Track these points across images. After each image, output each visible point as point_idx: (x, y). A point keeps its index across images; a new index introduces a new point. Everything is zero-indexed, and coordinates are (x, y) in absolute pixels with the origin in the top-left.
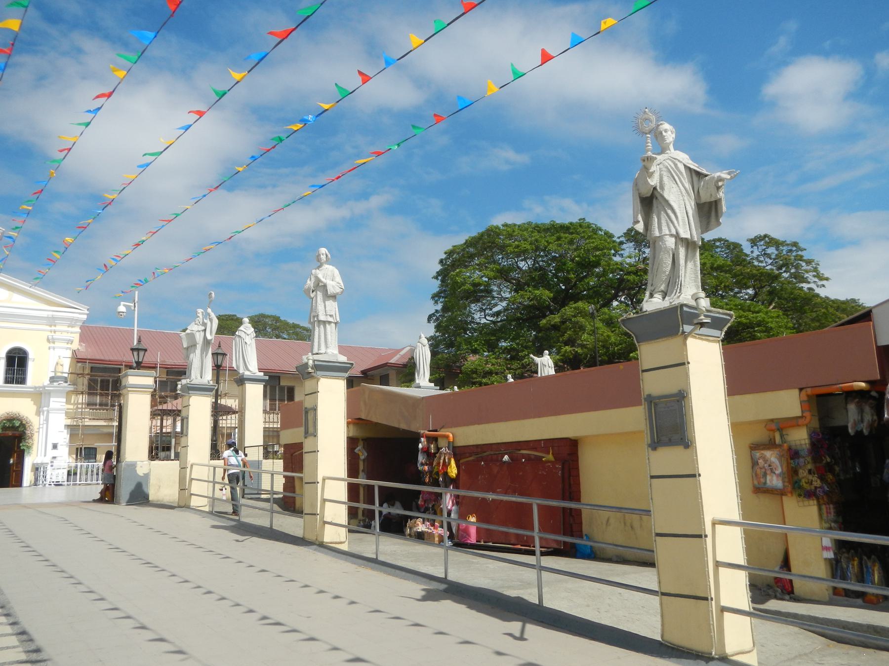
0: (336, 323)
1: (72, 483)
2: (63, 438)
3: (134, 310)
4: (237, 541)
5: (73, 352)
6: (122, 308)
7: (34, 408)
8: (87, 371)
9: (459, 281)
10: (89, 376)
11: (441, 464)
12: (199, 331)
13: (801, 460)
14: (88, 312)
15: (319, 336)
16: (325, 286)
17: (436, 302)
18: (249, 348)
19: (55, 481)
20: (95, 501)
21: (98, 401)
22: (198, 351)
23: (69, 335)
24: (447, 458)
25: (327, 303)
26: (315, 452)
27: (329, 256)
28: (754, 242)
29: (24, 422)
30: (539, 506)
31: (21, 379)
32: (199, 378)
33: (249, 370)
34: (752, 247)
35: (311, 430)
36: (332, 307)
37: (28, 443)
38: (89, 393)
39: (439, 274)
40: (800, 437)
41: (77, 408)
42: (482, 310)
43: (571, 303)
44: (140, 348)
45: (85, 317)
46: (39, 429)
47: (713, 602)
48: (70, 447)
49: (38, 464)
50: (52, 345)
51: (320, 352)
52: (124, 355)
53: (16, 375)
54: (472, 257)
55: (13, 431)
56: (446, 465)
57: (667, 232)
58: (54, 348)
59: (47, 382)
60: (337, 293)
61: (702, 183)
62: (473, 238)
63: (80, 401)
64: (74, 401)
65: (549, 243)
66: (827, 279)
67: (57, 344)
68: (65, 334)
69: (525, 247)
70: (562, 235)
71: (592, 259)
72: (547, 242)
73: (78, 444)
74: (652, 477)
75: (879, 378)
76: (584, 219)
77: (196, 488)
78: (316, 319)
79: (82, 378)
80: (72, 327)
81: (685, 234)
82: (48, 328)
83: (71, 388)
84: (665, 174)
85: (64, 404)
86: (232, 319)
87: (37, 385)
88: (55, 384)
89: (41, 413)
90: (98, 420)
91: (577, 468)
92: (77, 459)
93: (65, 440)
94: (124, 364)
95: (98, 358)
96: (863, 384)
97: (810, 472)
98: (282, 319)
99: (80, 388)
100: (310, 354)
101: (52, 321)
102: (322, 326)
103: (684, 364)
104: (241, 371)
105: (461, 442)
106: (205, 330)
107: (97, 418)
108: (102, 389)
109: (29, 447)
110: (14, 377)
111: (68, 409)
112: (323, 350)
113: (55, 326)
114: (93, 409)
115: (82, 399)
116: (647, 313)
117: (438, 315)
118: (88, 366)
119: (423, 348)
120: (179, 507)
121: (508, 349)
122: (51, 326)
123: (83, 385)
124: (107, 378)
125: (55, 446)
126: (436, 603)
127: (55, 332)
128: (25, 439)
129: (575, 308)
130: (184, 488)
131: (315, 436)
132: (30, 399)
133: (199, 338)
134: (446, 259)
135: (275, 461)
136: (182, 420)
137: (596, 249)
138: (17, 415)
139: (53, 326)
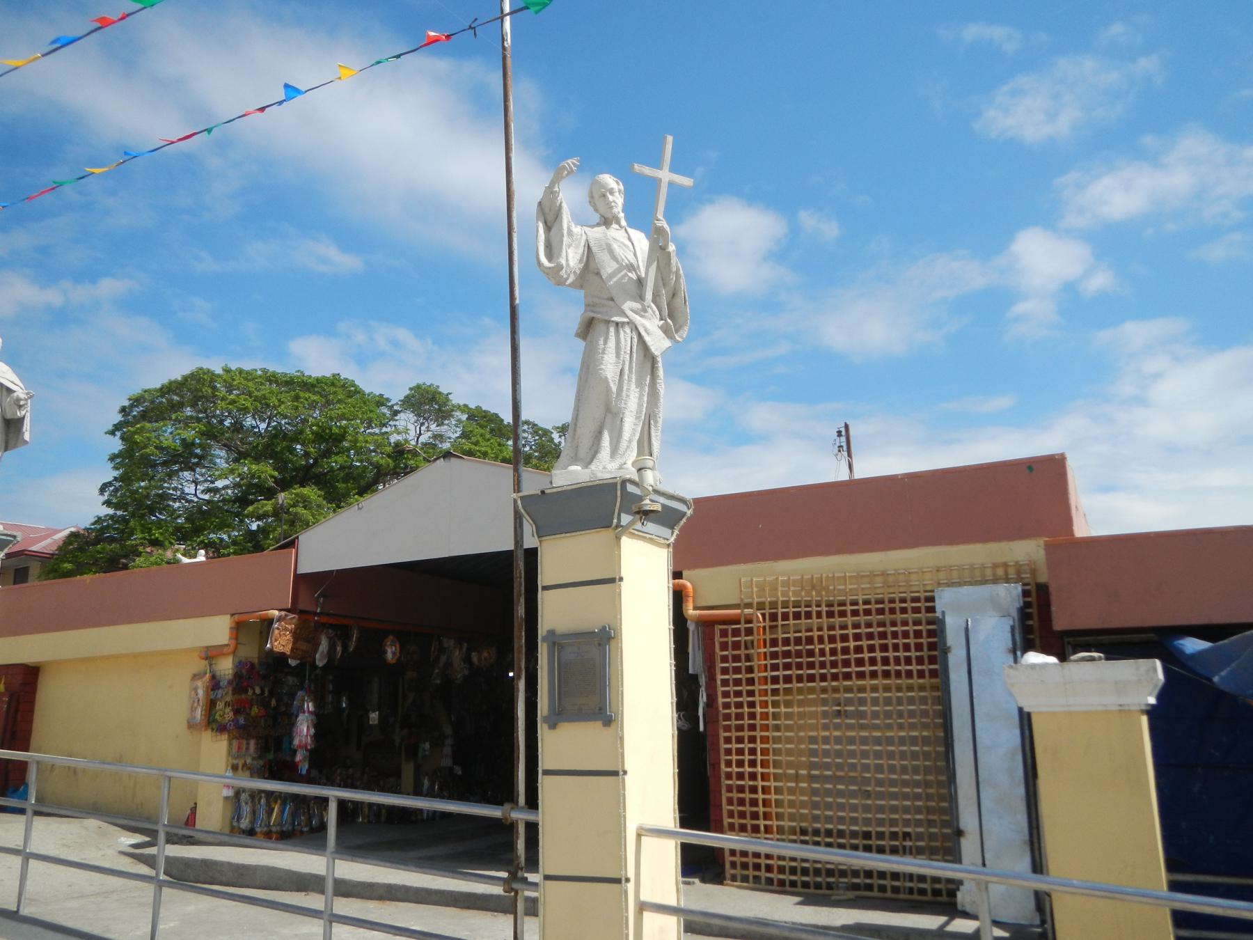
9: (138, 440)
13: (220, 692)
39: (117, 427)
40: (226, 667)
42: (196, 482)
43: (295, 486)
54: (179, 406)
69: (244, 405)
70: (302, 394)
71: (335, 430)
72: (279, 400)
76: (339, 374)
97: (228, 704)
121: (206, 543)
129: (297, 495)
134: (132, 406)
137: (342, 417)
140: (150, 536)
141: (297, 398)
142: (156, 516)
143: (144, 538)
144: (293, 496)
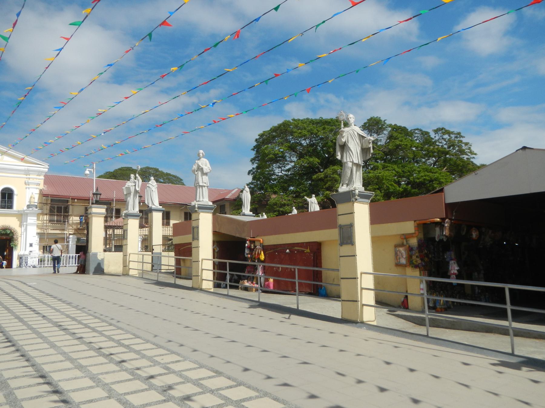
0: (207, 187)
1: (43, 266)
2: (35, 240)
3: (94, 173)
4: (160, 288)
5: (40, 190)
6: (87, 172)
7: (18, 223)
8: (49, 202)
10: (50, 205)
11: (257, 254)
12: (132, 186)
13: (414, 252)
14: (48, 167)
15: (199, 192)
16: (202, 169)
17: (253, 163)
18: (154, 193)
19: (33, 265)
20: (74, 273)
21: (56, 219)
22: (132, 196)
23: (38, 180)
24: (259, 251)
25: (203, 177)
26: (198, 247)
27: (204, 154)
28: (436, 131)
29: (12, 231)
30: (298, 269)
31: (10, 206)
32: (132, 209)
33: (154, 205)
34: (435, 134)
35: (195, 237)
36: (205, 178)
37: (15, 243)
38: (50, 214)
39: (255, 147)
40: (414, 242)
41: (44, 223)
42: (279, 167)
43: (331, 166)
44: (98, 193)
45: (47, 170)
46: (21, 235)
47: (359, 302)
48: (40, 246)
49: (21, 255)
50: (28, 186)
51: (200, 200)
52: (71, 192)
53: (7, 204)
54: (274, 137)
55: (6, 236)
56: (259, 254)
57: (349, 160)
58: (29, 188)
59: (25, 208)
60: (208, 172)
61: (364, 140)
62: (275, 127)
63: (45, 219)
64: (42, 219)
65: (319, 131)
66: (476, 154)
67: (30, 186)
68: (35, 180)
69: (305, 134)
72: (317, 130)
73: (43, 244)
74: (340, 257)
75: (445, 217)
77: (132, 265)
78: (198, 185)
79: (46, 206)
80: (39, 176)
81: (356, 161)
82: (25, 176)
83: (40, 211)
84: (349, 136)
85: (36, 221)
86: (130, 170)
87: (19, 210)
88: (30, 209)
89: (22, 226)
90: (55, 230)
91: (320, 256)
92: (44, 252)
93: (37, 241)
94: (71, 198)
95: (55, 194)
96: (439, 220)
97: (417, 257)
98: (160, 170)
99: (45, 212)
100: (195, 201)
101: (27, 172)
102: (201, 188)
103: (352, 213)
104: (150, 206)
105: (266, 244)
106: (135, 186)
107: (55, 229)
108: (58, 212)
109: (16, 246)
110: (5, 205)
111: (38, 224)
112: (201, 200)
113: (29, 175)
114: (53, 224)
115: (46, 218)
116: (340, 193)
117: (254, 170)
118: (50, 198)
119: (247, 193)
120: (123, 275)
121: (295, 192)
122: (27, 175)
123: (47, 210)
124: (61, 206)
125: (31, 245)
126: (255, 309)
127: (29, 178)
128: (13, 241)
129: (333, 169)
130: (125, 265)
131: (198, 240)
132: (16, 218)
133: (132, 190)
134: (259, 139)
135: (169, 253)
136: (124, 231)
138: (8, 227)
139: (28, 175)
140: (274, 190)
141: (324, 129)
142: (271, 182)
143: (271, 191)
144: (331, 170)
